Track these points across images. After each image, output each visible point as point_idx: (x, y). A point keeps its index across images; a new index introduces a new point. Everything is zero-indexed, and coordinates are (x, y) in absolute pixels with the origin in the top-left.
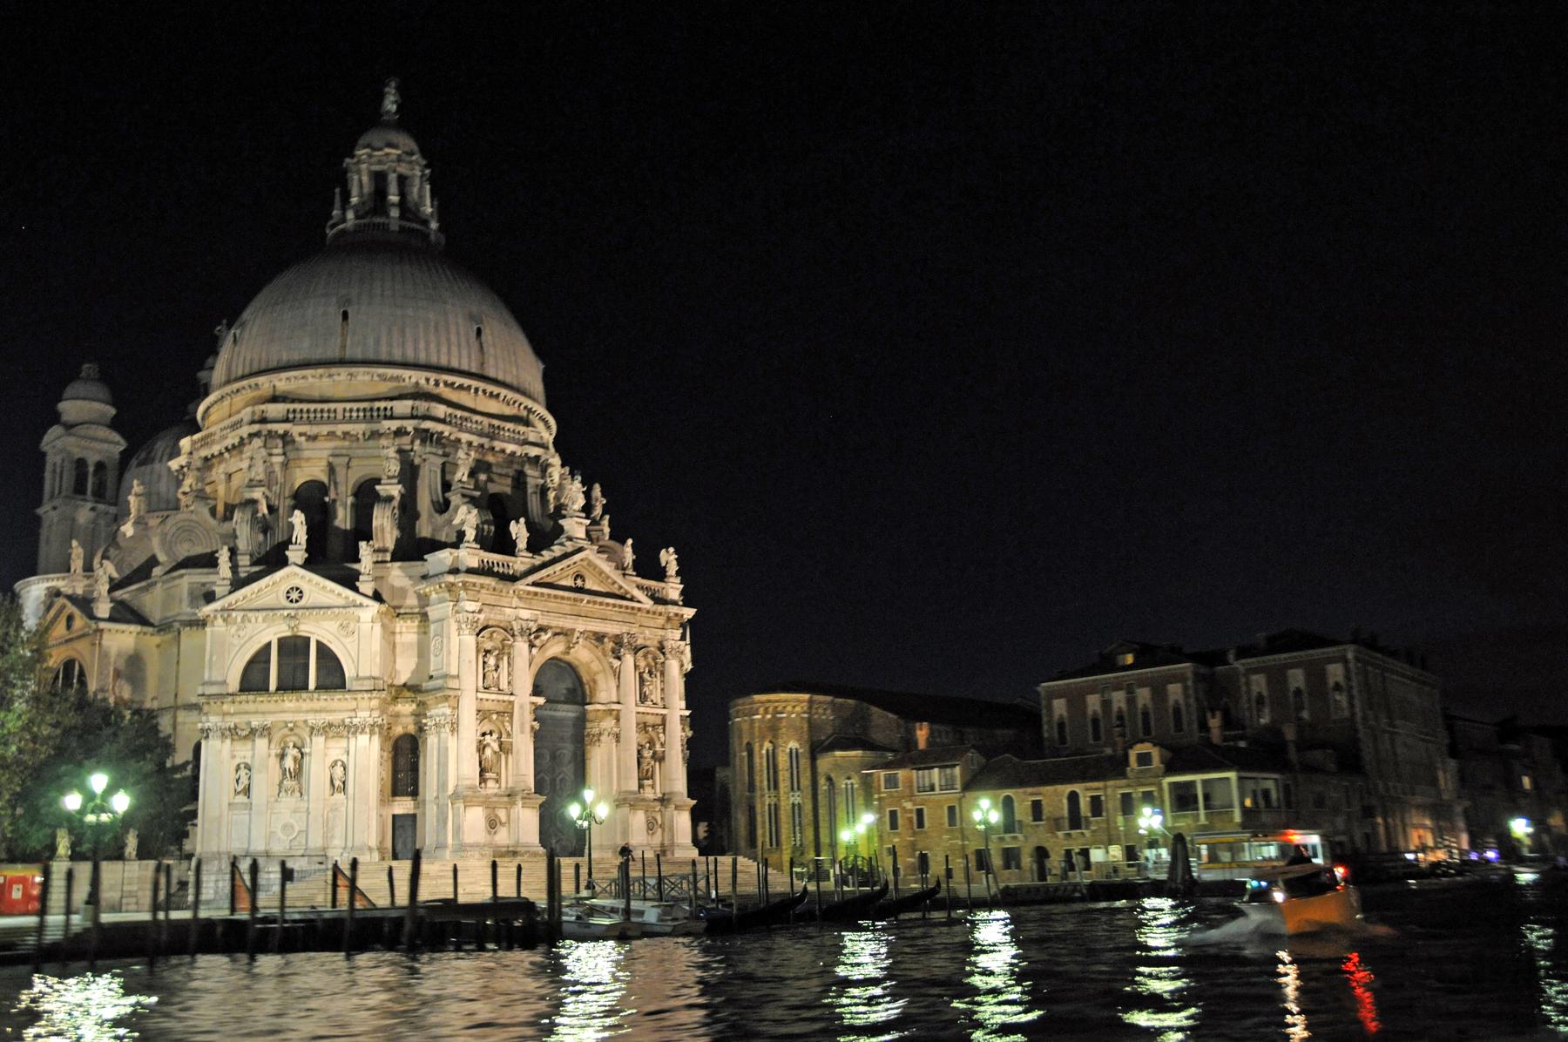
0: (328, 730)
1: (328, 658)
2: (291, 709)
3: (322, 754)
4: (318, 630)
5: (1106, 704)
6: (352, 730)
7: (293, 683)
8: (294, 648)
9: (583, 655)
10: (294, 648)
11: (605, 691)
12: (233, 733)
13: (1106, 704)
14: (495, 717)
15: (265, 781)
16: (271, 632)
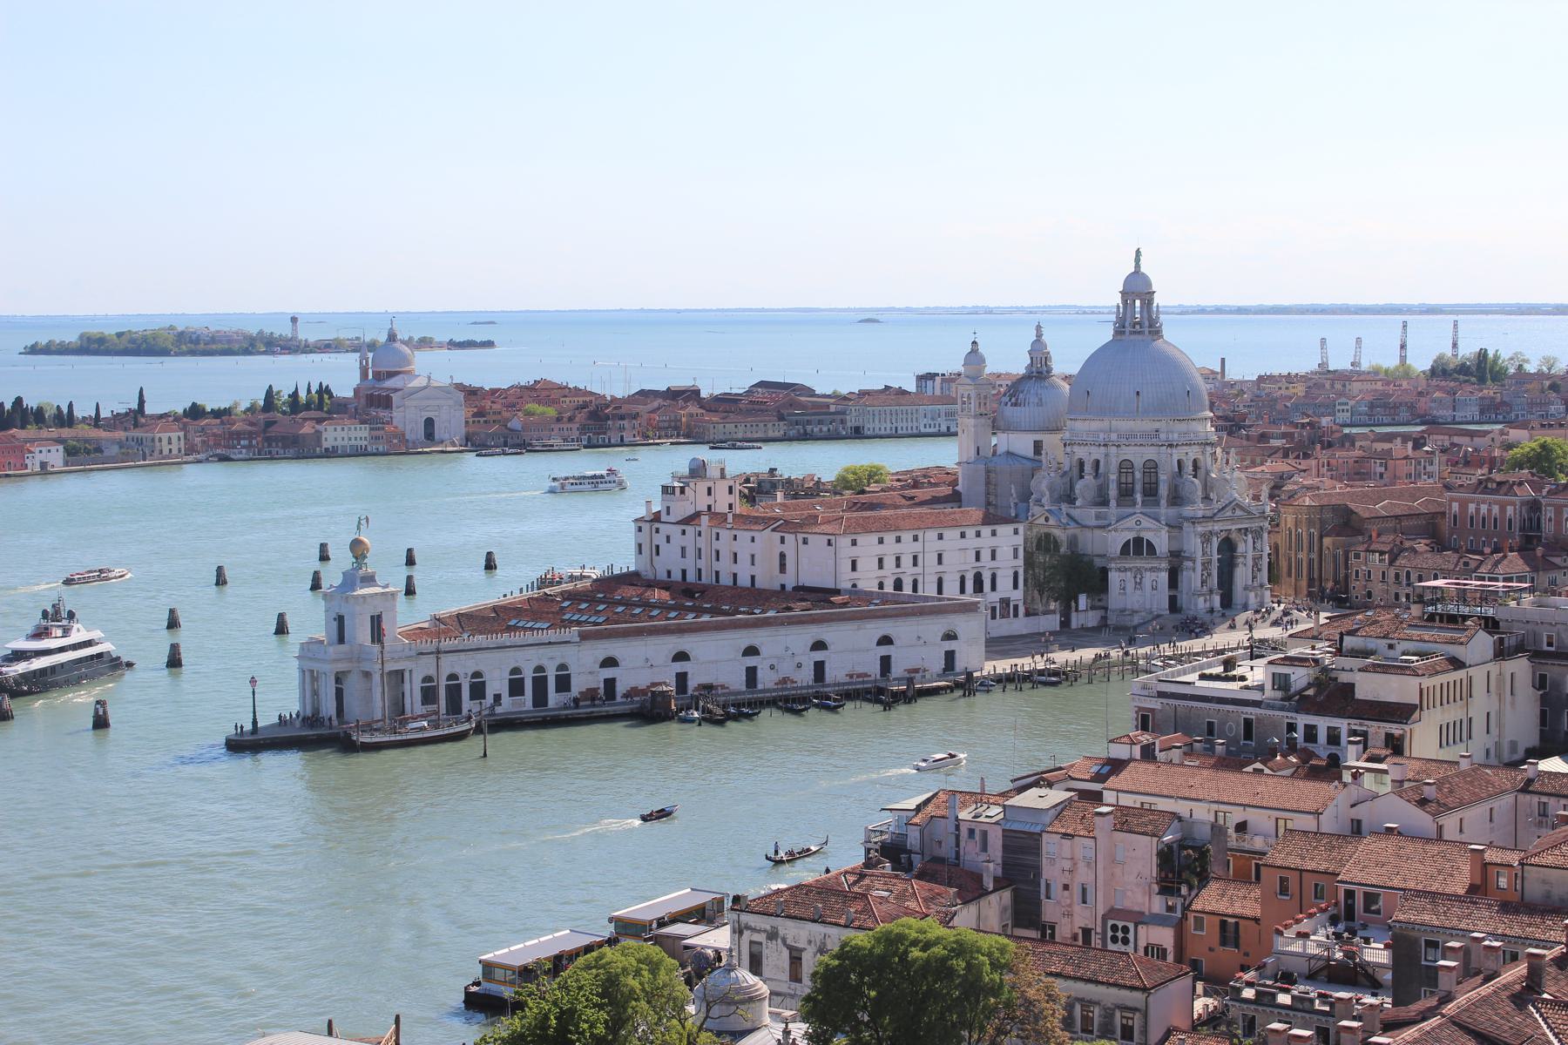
0: (1152, 569)
1: (1150, 544)
2: (1139, 563)
3: (1148, 577)
4: (1146, 535)
5: (1478, 510)
6: (1159, 570)
7: (1138, 552)
8: (1138, 541)
9: (1233, 536)
10: (1138, 541)
11: (1241, 548)
12: (1119, 570)
13: (1478, 510)
14: (1206, 565)
15: (1130, 586)
16: (1130, 536)
